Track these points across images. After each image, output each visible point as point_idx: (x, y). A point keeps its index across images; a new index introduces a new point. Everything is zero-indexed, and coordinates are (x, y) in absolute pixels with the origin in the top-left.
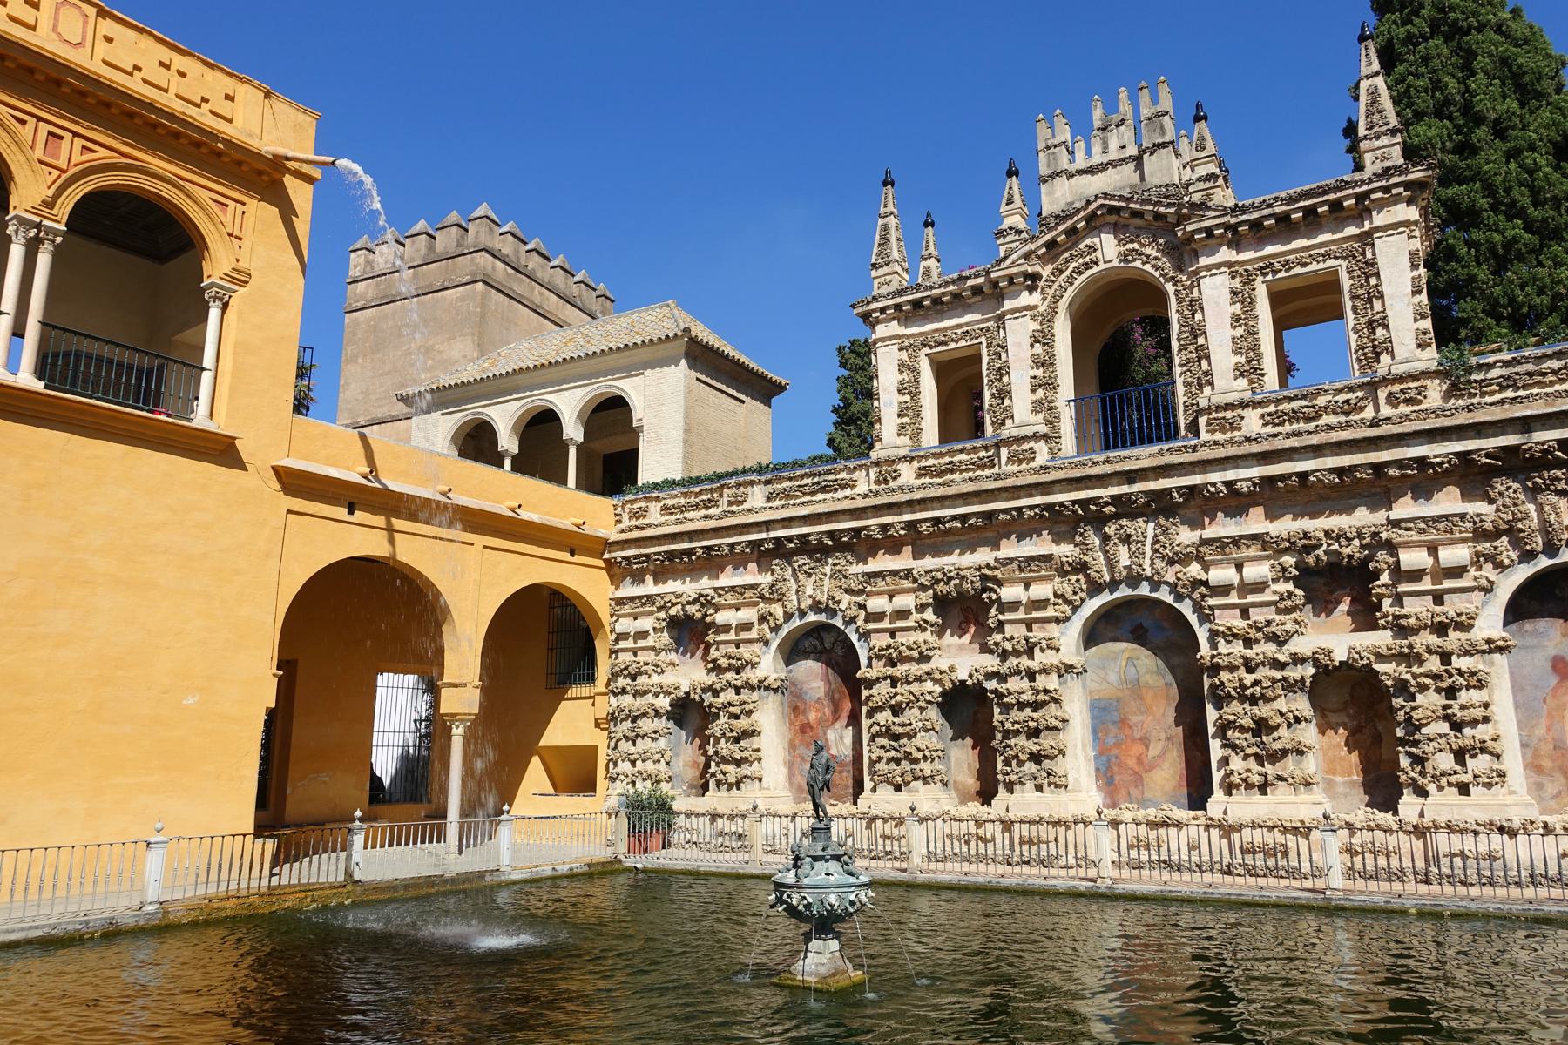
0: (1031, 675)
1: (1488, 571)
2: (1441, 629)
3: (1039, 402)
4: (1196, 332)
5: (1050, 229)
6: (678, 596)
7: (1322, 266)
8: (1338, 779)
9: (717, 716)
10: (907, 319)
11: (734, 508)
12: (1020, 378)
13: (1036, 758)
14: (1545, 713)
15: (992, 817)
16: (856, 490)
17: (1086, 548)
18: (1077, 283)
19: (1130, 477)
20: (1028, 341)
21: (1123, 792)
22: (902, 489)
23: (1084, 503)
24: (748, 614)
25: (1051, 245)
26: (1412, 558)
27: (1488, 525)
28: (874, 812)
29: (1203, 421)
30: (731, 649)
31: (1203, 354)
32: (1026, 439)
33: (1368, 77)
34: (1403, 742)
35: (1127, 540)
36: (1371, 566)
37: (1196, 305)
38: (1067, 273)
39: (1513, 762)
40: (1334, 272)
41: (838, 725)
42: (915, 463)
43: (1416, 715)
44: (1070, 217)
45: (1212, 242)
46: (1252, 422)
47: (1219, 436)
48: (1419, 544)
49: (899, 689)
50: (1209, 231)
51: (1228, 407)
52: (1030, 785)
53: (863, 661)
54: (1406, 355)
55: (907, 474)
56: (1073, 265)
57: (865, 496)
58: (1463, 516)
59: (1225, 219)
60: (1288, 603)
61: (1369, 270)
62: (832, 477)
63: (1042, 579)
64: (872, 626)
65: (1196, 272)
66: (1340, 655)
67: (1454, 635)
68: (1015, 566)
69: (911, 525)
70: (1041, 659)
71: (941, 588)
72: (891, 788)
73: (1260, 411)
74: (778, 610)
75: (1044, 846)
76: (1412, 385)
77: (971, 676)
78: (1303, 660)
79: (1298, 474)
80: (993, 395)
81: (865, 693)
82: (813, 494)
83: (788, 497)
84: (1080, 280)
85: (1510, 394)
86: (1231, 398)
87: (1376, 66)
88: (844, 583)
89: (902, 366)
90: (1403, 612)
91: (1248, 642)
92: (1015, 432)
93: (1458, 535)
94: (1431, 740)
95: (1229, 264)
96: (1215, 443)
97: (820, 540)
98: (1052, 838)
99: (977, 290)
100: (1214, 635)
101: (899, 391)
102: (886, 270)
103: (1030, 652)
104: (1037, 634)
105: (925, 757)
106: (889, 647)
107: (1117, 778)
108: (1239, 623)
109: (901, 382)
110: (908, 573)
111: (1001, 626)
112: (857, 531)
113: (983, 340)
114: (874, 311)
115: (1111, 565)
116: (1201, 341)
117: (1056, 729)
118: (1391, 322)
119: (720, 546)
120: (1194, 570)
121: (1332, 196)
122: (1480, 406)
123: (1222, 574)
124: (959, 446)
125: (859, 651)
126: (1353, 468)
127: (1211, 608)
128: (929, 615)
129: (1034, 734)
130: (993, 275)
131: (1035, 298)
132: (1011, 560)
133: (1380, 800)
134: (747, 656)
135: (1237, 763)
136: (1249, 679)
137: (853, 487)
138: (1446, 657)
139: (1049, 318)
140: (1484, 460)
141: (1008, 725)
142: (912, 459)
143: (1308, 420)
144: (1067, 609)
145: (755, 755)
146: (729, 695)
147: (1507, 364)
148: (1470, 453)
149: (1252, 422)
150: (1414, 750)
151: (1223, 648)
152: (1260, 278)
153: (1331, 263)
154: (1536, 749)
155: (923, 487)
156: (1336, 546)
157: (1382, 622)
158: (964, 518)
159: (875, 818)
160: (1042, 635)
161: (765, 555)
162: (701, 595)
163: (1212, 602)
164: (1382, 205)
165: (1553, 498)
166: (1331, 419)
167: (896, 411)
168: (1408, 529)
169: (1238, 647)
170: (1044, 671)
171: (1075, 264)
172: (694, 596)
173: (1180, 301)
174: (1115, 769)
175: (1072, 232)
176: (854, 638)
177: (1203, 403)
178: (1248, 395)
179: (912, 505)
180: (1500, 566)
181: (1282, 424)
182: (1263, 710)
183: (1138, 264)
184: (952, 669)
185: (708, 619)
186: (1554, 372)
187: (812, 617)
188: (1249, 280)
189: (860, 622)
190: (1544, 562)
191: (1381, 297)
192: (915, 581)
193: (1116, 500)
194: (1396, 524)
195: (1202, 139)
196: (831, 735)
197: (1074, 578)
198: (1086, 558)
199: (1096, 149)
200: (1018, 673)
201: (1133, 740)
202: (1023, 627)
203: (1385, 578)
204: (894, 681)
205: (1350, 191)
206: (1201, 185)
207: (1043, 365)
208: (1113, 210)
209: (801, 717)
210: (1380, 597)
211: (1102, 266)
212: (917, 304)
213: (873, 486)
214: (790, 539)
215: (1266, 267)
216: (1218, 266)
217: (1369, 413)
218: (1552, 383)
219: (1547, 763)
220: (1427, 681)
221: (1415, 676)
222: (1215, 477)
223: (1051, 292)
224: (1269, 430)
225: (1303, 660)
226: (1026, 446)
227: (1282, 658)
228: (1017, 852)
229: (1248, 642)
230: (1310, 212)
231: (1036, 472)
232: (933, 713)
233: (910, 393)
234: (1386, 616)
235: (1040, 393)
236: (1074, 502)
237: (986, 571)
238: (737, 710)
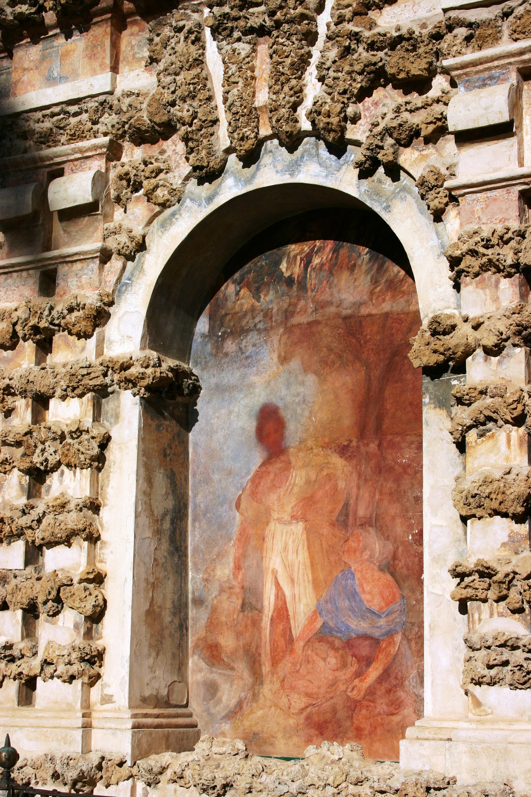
14: (235, 531)
58: (105, 104)
154: (214, 610)
219: (227, 641)
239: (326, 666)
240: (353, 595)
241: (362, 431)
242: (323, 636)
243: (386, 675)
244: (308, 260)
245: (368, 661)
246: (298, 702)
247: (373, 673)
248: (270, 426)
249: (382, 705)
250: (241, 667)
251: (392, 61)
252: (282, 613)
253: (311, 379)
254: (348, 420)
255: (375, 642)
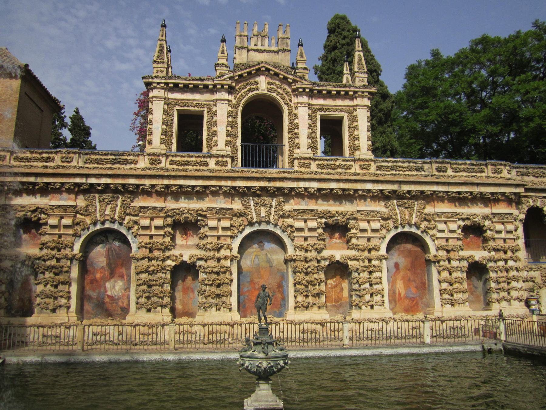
0: (219, 260)
1: (384, 231)
2: (370, 251)
3: (230, 142)
4: (294, 127)
5: (242, 70)
6: (23, 207)
7: (340, 113)
8: (328, 304)
9: (43, 273)
10: (169, 91)
11: (65, 164)
12: (222, 129)
13: (218, 296)
15: (196, 323)
16: (137, 166)
17: (248, 208)
18: (249, 95)
19: (270, 179)
20: (226, 115)
21: (249, 311)
22: (162, 169)
23: (249, 188)
24: (66, 221)
25: (240, 76)
26: (363, 225)
27: (386, 216)
28: (136, 322)
29: (296, 162)
30: (56, 238)
31: (297, 136)
32: (223, 156)
33: (359, 51)
34: (356, 290)
35: (264, 205)
36: (349, 226)
37: (296, 116)
38: (246, 90)
39: (386, 299)
40: (343, 117)
41: (112, 280)
42: (170, 158)
43: (361, 281)
44: (250, 67)
45: (304, 93)
46: (314, 167)
47: (303, 169)
48: (364, 220)
49: (154, 262)
50: (304, 89)
51: (305, 159)
52: (214, 308)
53: (134, 247)
54: (365, 152)
55: (164, 163)
56: (248, 87)
57: (143, 169)
58: (378, 212)
59: (311, 86)
60: (322, 238)
61: (353, 119)
62: (122, 157)
63: (226, 218)
64: (141, 232)
65: (297, 103)
66: (338, 258)
67: (373, 253)
68: (214, 211)
69: (167, 187)
70: (224, 253)
71: (177, 217)
72: (144, 310)
73: (317, 162)
74: (88, 221)
75: (219, 335)
76: (366, 163)
77: (190, 259)
78: (325, 259)
79: (330, 189)
80: (208, 134)
81: (133, 266)
82: (113, 164)
83: (98, 164)
84: (251, 94)
85: (394, 172)
86: (307, 156)
87: (360, 48)
88: (128, 212)
89: (165, 112)
90: (358, 244)
91: (306, 251)
92: (219, 153)
93: (377, 218)
94: (364, 290)
95: (309, 104)
96: (301, 172)
97: (116, 188)
98: (223, 331)
99: (206, 86)
100: (296, 248)
101: (163, 123)
102: (160, 65)
103: (218, 250)
104: (222, 241)
105: (164, 296)
106: (150, 243)
107: (247, 305)
108: (305, 244)
109: (164, 119)
110: (162, 209)
111: (206, 236)
112: (138, 186)
113: (206, 109)
114: (155, 83)
115: (258, 215)
116: (296, 131)
117: (228, 283)
118: (360, 139)
119: (55, 183)
120: (290, 221)
121: (347, 89)
122: (386, 175)
123: (299, 224)
124: (191, 154)
125: (132, 244)
126: (348, 190)
127: (294, 237)
128: (169, 229)
129: (219, 286)
130: (216, 82)
131: (231, 97)
132: (214, 208)
133: (341, 312)
134: (66, 242)
135: (300, 298)
136: (307, 265)
137: (136, 164)
138: (370, 261)
139: (236, 107)
140: (387, 194)
141: (206, 282)
142: (167, 156)
143: (333, 169)
144: (236, 231)
145: (67, 295)
146: (53, 262)
147: (393, 162)
148: (383, 190)
149: (314, 167)
150: (358, 293)
151: (298, 253)
152: (319, 113)
153: (343, 113)
155: (173, 170)
156: (339, 218)
157: (351, 247)
158: (193, 187)
159: (137, 325)
160: (225, 243)
161: (78, 190)
162: (38, 208)
163: (295, 234)
164: (363, 97)
165: (404, 209)
166: (339, 170)
167: (160, 131)
168: (362, 214)
169: (303, 253)
170: (225, 258)
171: (248, 87)
172: (34, 208)
173: (290, 114)
174: (247, 301)
175: (249, 73)
176: (130, 238)
177: (296, 156)
178: (312, 156)
179: (169, 177)
180: (387, 230)
181: (324, 168)
182: (309, 278)
183: (274, 95)
184: (181, 256)
185: (41, 222)
186: (405, 168)
187: (107, 225)
188: (315, 112)
189: (134, 230)
190: (400, 230)
191: (358, 130)
192: (166, 213)
193: (262, 189)
194: (358, 211)
195: (301, 53)
196: (108, 285)
197: (241, 219)
198: (247, 211)
199: (259, 43)
200: (212, 258)
201: (255, 289)
202: (216, 239)
203: (353, 231)
204: (150, 259)
205: (353, 89)
206: (302, 71)
207: (232, 127)
208: (268, 70)
209: (91, 276)
210: (351, 237)
211: (260, 91)
212: (176, 85)
213: (148, 165)
214: (99, 185)
215: (322, 108)
216: (305, 104)
217: (352, 171)
218: (405, 171)
220: (365, 269)
221: (361, 267)
222: (302, 185)
223: (238, 96)
224: (319, 170)
225: (325, 259)
226: (225, 159)
227: (319, 258)
228: (206, 338)
229: (306, 251)
230: (338, 92)
231: (228, 172)
232: (169, 276)
233: (167, 125)
234: (353, 244)
235: (229, 139)
236: (245, 187)
237: (200, 212)
238: (56, 271)
239: (407, 302)
240: (411, 291)
241: (412, 267)
242: (406, 297)
243: (416, 303)
244: (402, 240)
245: (413, 301)
246: (403, 307)
247: (414, 302)
248: (397, 265)
249: (416, 307)
250: (393, 302)
251: (427, 217)
252: (400, 294)
253: (403, 259)
254: (409, 265)
255: (415, 298)
